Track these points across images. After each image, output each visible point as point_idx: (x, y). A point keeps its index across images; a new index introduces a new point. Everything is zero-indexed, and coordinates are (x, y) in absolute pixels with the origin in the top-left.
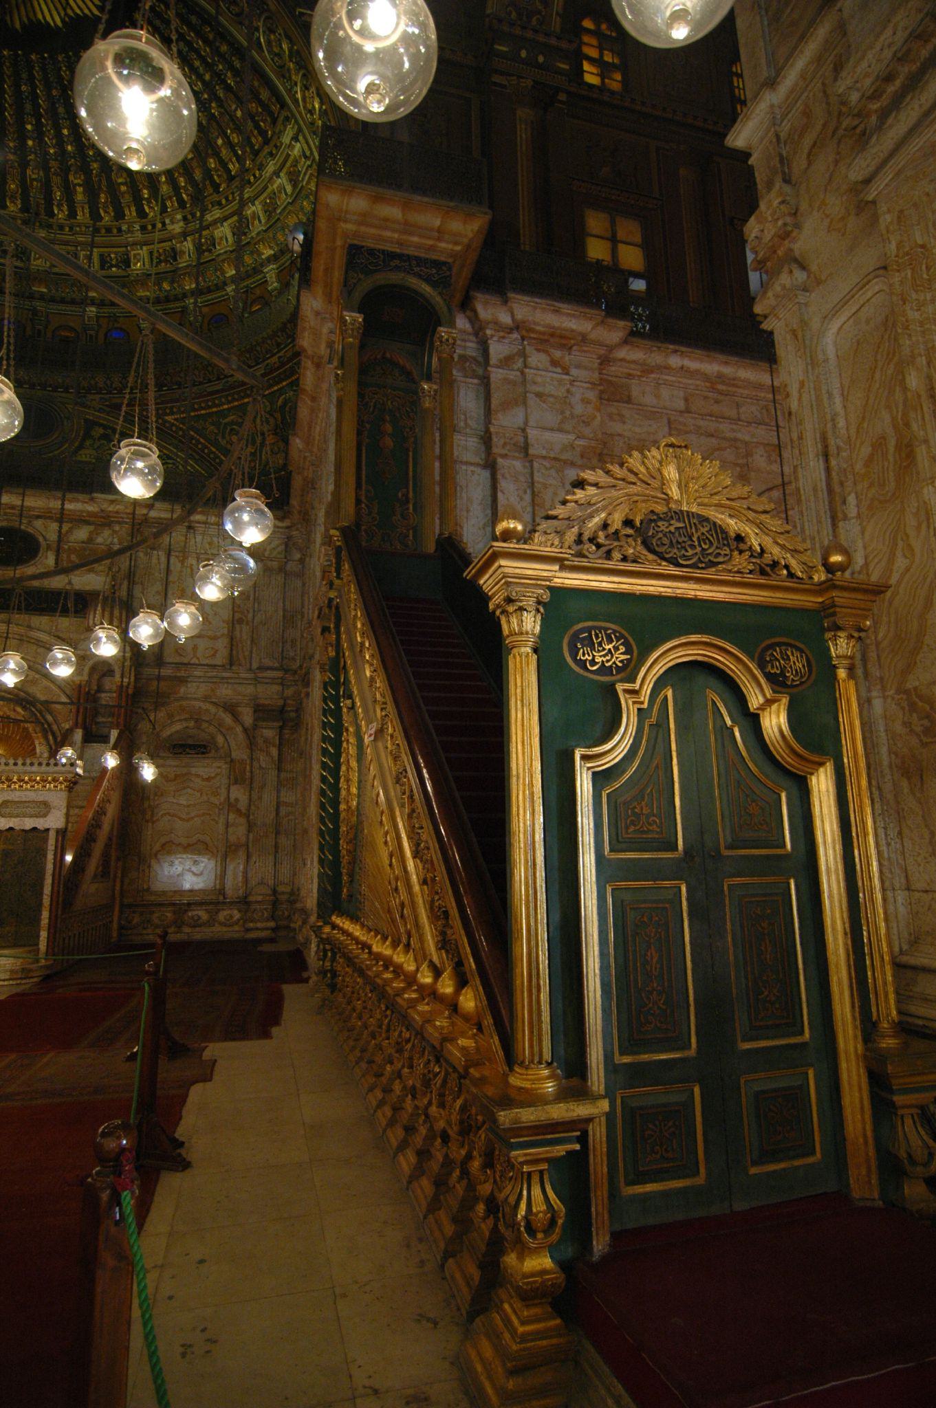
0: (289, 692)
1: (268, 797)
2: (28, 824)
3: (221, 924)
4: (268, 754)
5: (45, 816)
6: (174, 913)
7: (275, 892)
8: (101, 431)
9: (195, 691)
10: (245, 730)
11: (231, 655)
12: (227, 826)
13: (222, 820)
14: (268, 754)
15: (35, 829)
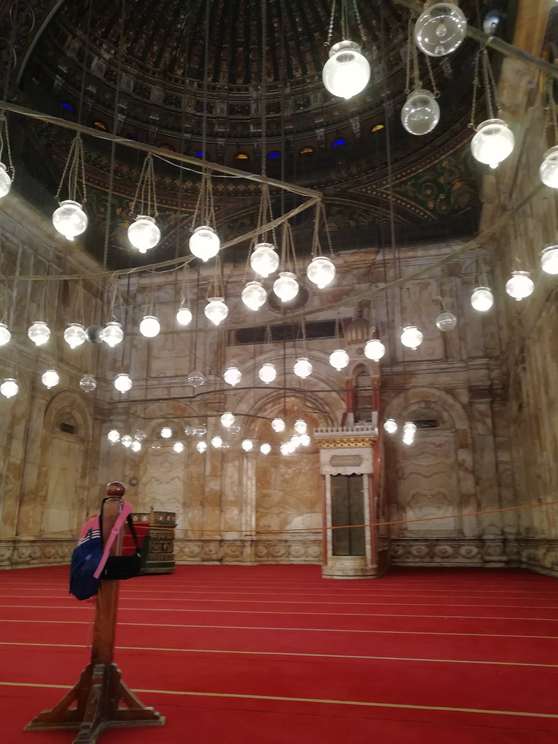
0: (495, 373)
1: (489, 458)
2: (349, 471)
3: (464, 557)
4: (484, 424)
5: (359, 465)
6: (427, 546)
7: (503, 533)
8: (337, 209)
9: (421, 380)
10: (464, 406)
11: (445, 351)
12: (459, 481)
13: (454, 476)
14: (484, 424)
15: (354, 475)
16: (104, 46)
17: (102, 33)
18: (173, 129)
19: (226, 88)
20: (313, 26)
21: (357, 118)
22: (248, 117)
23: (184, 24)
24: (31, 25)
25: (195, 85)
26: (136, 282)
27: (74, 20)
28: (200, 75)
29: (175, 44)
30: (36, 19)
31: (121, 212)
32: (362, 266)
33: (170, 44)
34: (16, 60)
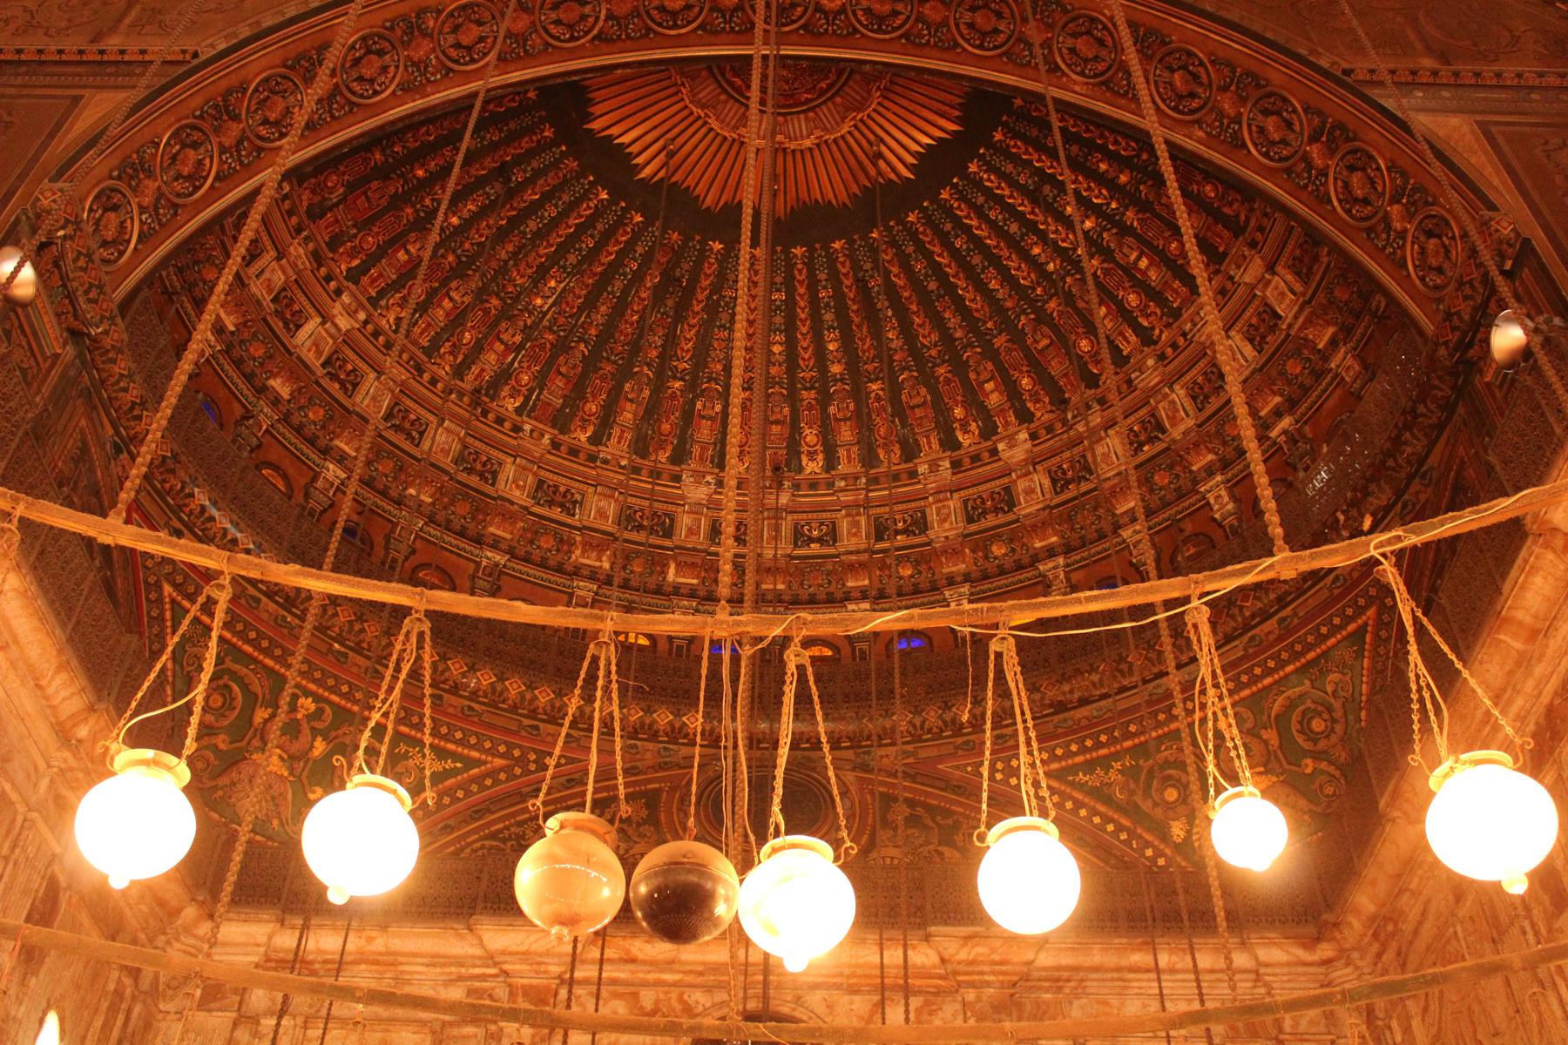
16: (346, 298)
17: (349, 270)
18: (462, 533)
19: (624, 463)
20: (870, 367)
21: (965, 589)
22: (668, 543)
23: (551, 301)
24: (200, 187)
25: (546, 440)
26: (263, 939)
27: (294, 220)
28: (561, 421)
29: (518, 339)
30: (217, 178)
31: (266, 721)
32: (991, 978)
33: (505, 337)
34: (132, 246)
